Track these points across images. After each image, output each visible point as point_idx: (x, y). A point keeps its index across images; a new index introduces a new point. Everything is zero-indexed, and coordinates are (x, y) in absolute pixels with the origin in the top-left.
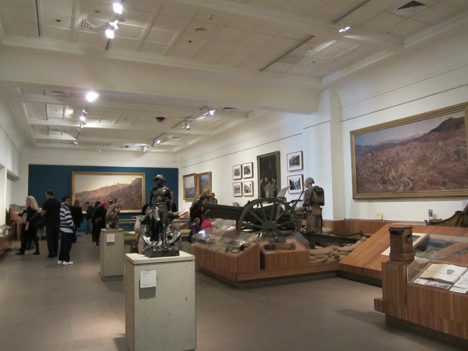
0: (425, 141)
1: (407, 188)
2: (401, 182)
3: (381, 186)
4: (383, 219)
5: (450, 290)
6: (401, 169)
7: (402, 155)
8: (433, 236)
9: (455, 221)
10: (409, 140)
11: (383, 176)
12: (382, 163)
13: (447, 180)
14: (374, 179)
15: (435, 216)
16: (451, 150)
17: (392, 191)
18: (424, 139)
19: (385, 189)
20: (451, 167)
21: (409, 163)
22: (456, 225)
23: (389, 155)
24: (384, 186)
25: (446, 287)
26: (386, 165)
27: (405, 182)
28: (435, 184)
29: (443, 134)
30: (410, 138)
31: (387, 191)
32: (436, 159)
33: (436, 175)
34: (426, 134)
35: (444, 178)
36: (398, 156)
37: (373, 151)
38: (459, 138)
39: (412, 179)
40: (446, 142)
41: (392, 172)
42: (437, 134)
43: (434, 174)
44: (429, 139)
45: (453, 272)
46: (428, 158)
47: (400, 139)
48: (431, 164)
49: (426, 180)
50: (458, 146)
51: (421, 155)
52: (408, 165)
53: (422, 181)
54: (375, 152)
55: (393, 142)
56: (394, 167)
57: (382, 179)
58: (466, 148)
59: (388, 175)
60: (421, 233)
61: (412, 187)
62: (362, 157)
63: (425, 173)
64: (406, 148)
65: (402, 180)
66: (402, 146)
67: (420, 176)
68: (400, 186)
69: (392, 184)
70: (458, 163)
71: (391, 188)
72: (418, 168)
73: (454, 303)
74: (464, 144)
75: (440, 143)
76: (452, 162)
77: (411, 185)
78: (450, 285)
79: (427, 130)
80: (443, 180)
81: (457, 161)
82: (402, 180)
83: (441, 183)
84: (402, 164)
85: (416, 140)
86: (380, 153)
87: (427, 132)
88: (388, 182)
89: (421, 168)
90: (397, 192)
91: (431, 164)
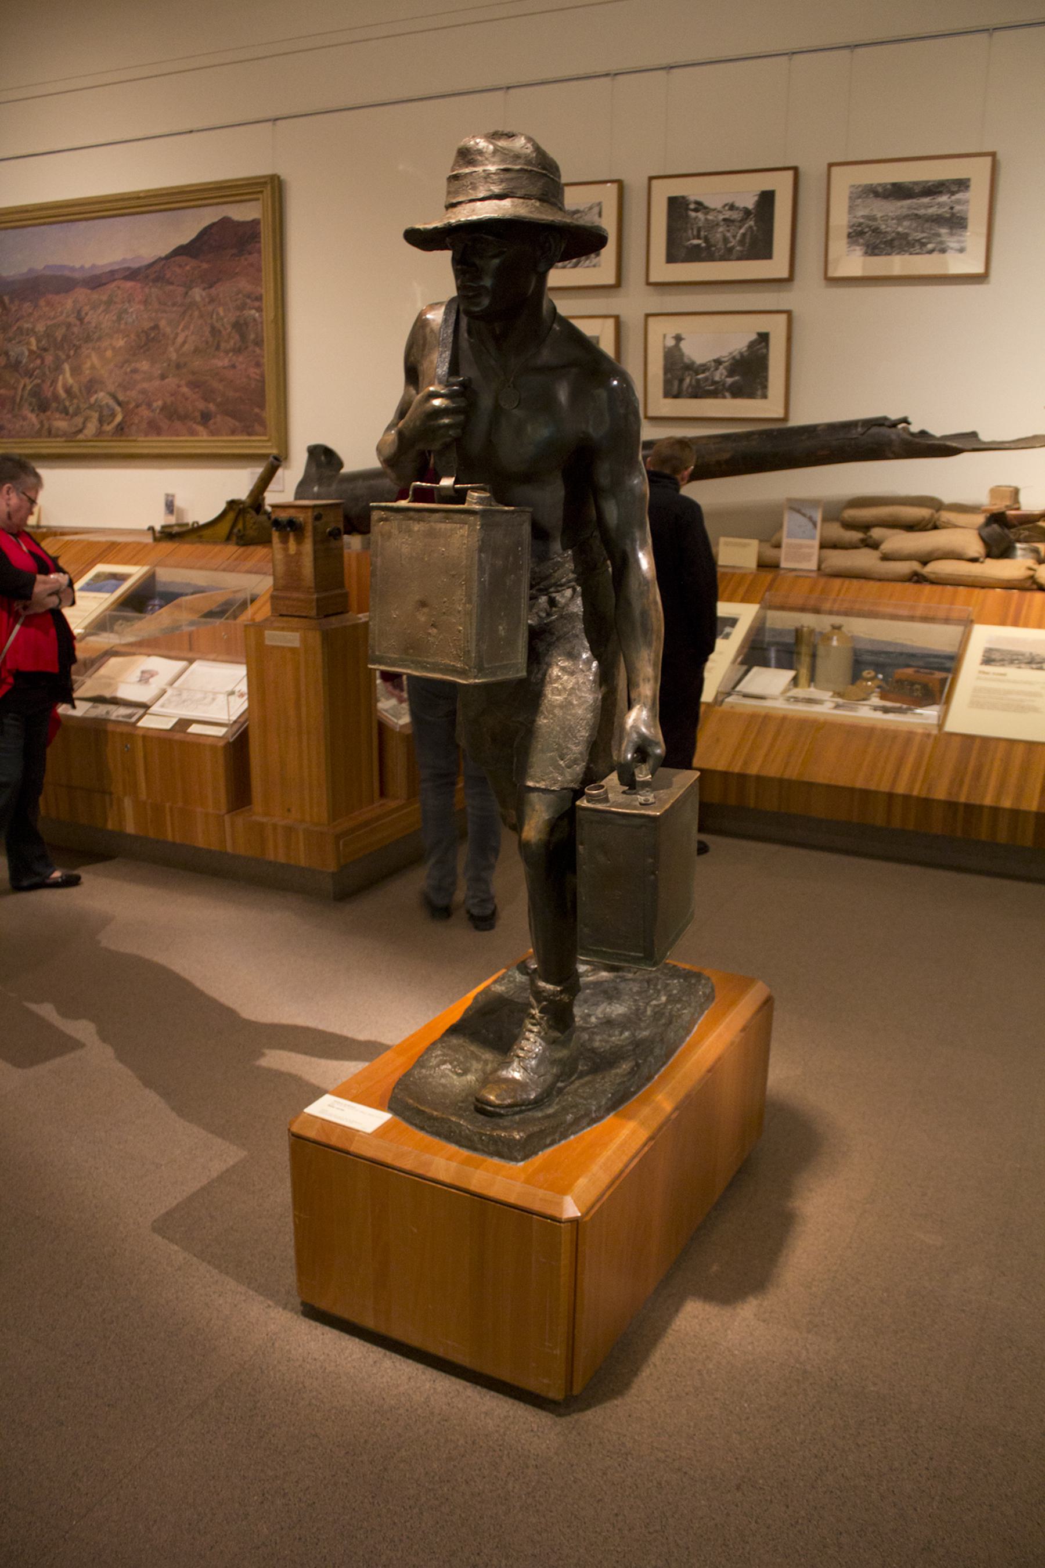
0: (156, 280)
1: (108, 428)
2: (91, 407)
3: (32, 417)
4: (43, 523)
5: (140, 724)
6: (88, 365)
7: (92, 318)
8: (166, 576)
9: (224, 528)
10: (112, 272)
11: (38, 385)
12: (33, 341)
13: (212, 407)
15: (181, 512)
16: (225, 316)
17: (65, 434)
18: (150, 274)
19: (46, 426)
20: (224, 368)
21: (114, 348)
22: (228, 539)
23: (54, 318)
24: (42, 416)
25: (130, 716)
26: (45, 350)
27: (100, 406)
28: (184, 418)
29: (205, 266)
30: (117, 267)
31: (50, 432)
32: (184, 342)
33: (185, 390)
34: (161, 259)
35: (206, 400)
36: (81, 320)
38: (244, 284)
39: (121, 398)
40: (213, 291)
41: (63, 372)
42: (190, 264)
43: (179, 386)
44: (168, 276)
45: (152, 676)
46: (164, 335)
47: (87, 266)
48: (174, 356)
49: (160, 403)
50: (242, 307)
51: (147, 325)
52: (109, 353)
53: (149, 405)
54: (12, 301)
55: (67, 273)
56: (68, 357)
57: (36, 393)
58: (261, 316)
59: (54, 382)
60: (135, 564)
61: (119, 424)
63: (157, 383)
64: (104, 298)
65: (92, 400)
66: (93, 289)
67: (144, 392)
68: (86, 419)
69: (65, 411)
70: (241, 359)
71: (61, 424)
72: (138, 365)
73: (145, 757)
74: (257, 304)
75: (198, 294)
76: (227, 352)
77: (119, 418)
78: (141, 711)
79: (164, 249)
80: (201, 405)
81: (238, 351)
82: (92, 400)
83: (197, 414)
84: (93, 349)
85: (132, 274)
86: (27, 306)
87: (163, 255)
88: (54, 405)
89: (144, 365)
90: (81, 437)
91: (174, 356)
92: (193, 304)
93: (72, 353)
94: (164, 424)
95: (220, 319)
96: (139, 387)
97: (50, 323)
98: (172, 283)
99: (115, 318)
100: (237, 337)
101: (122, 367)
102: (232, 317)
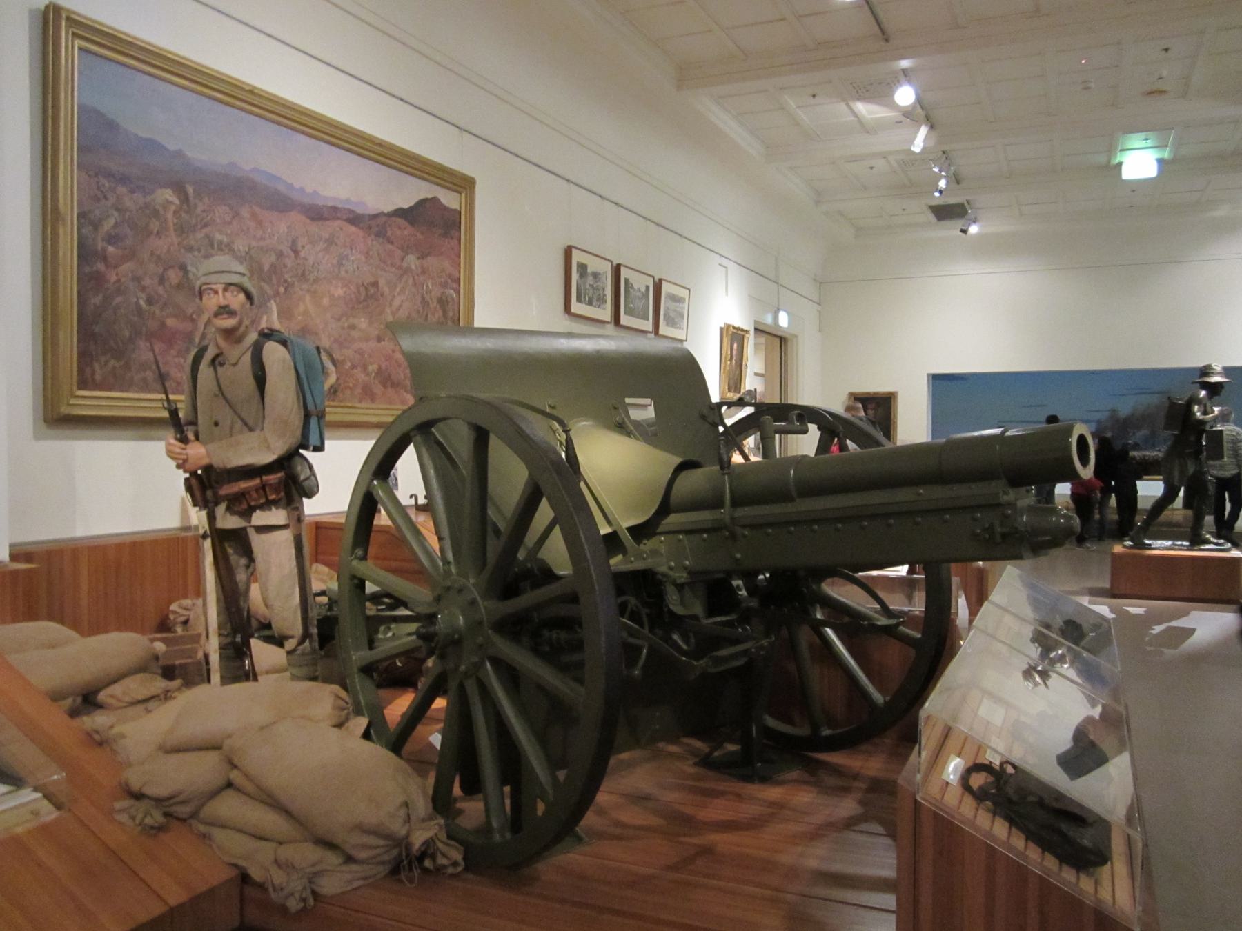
6: (302, 308)
10: (335, 209)
14: (188, 326)
23: (262, 239)
29: (420, 236)
34: (382, 214)
36: (296, 252)
37: (190, 190)
41: (268, 312)
43: (393, 351)
47: (309, 190)
49: (375, 367)
52: (326, 301)
55: (281, 188)
56: (277, 294)
62: (122, 190)
63: (373, 344)
66: (313, 219)
67: (360, 352)
72: (355, 321)
75: (412, 261)
77: (332, 379)
84: (308, 291)
85: (355, 219)
86: (222, 212)
92: (407, 271)
93: (282, 290)
94: (378, 389)
95: (429, 292)
96: (356, 346)
97: (254, 244)
98: (392, 243)
99: (335, 262)
100: (440, 313)
101: (339, 320)
102: (437, 292)
